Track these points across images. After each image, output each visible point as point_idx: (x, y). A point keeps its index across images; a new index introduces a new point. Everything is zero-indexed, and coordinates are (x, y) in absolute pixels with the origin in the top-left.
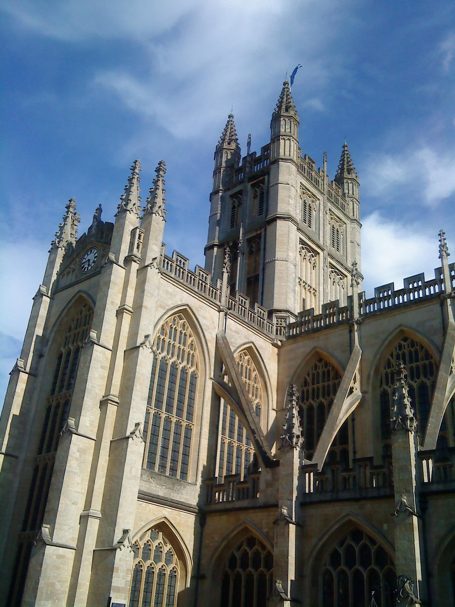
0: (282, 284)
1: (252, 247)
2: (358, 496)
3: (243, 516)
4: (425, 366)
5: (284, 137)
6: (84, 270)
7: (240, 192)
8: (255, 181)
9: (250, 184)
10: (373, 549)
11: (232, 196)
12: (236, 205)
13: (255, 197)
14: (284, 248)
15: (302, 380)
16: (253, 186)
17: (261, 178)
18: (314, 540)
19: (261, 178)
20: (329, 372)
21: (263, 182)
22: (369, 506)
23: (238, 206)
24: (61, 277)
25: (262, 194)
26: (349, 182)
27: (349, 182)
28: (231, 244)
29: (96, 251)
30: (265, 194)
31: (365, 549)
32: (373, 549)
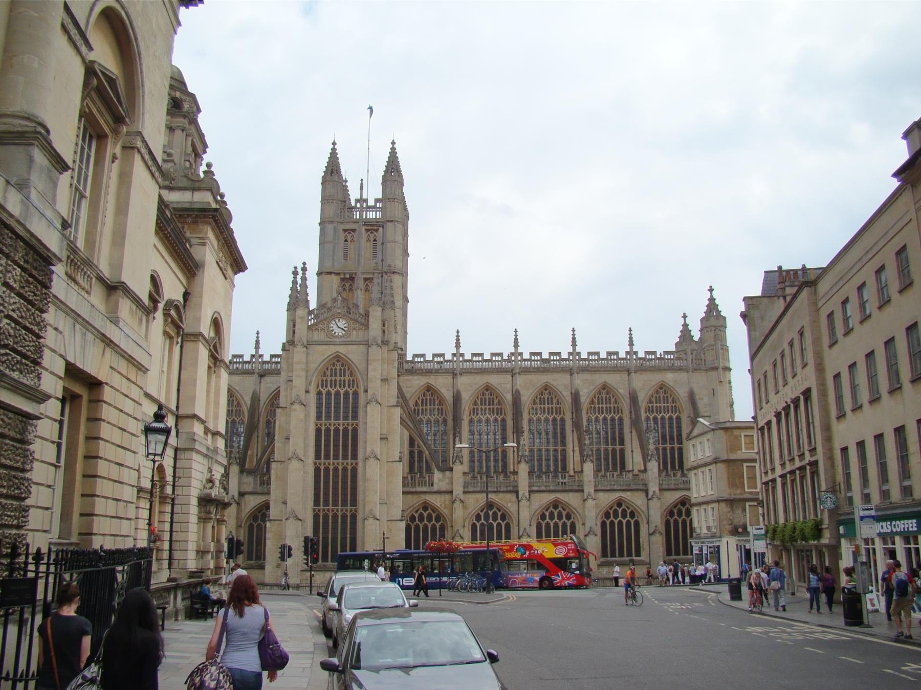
2: (495, 490)
3: (423, 497)
7: (354, 230)
8: (369, 228)
9: (364, 228)
10: (499, 514)
11: (345, 231)
12: (349, 240)
13: (368, 240)
15: (414, 401)
16: (367, 230)
17: (376, 228)
18: (470, 510)
19: (376, 228)
20: (434, 399)
21: (377, 230)
22: (501, 495)
25: (375, 240)
28: (348, 276)
29: (344, 322)
30: (379, 243)
31: (495, 514)
32: (499, 514)
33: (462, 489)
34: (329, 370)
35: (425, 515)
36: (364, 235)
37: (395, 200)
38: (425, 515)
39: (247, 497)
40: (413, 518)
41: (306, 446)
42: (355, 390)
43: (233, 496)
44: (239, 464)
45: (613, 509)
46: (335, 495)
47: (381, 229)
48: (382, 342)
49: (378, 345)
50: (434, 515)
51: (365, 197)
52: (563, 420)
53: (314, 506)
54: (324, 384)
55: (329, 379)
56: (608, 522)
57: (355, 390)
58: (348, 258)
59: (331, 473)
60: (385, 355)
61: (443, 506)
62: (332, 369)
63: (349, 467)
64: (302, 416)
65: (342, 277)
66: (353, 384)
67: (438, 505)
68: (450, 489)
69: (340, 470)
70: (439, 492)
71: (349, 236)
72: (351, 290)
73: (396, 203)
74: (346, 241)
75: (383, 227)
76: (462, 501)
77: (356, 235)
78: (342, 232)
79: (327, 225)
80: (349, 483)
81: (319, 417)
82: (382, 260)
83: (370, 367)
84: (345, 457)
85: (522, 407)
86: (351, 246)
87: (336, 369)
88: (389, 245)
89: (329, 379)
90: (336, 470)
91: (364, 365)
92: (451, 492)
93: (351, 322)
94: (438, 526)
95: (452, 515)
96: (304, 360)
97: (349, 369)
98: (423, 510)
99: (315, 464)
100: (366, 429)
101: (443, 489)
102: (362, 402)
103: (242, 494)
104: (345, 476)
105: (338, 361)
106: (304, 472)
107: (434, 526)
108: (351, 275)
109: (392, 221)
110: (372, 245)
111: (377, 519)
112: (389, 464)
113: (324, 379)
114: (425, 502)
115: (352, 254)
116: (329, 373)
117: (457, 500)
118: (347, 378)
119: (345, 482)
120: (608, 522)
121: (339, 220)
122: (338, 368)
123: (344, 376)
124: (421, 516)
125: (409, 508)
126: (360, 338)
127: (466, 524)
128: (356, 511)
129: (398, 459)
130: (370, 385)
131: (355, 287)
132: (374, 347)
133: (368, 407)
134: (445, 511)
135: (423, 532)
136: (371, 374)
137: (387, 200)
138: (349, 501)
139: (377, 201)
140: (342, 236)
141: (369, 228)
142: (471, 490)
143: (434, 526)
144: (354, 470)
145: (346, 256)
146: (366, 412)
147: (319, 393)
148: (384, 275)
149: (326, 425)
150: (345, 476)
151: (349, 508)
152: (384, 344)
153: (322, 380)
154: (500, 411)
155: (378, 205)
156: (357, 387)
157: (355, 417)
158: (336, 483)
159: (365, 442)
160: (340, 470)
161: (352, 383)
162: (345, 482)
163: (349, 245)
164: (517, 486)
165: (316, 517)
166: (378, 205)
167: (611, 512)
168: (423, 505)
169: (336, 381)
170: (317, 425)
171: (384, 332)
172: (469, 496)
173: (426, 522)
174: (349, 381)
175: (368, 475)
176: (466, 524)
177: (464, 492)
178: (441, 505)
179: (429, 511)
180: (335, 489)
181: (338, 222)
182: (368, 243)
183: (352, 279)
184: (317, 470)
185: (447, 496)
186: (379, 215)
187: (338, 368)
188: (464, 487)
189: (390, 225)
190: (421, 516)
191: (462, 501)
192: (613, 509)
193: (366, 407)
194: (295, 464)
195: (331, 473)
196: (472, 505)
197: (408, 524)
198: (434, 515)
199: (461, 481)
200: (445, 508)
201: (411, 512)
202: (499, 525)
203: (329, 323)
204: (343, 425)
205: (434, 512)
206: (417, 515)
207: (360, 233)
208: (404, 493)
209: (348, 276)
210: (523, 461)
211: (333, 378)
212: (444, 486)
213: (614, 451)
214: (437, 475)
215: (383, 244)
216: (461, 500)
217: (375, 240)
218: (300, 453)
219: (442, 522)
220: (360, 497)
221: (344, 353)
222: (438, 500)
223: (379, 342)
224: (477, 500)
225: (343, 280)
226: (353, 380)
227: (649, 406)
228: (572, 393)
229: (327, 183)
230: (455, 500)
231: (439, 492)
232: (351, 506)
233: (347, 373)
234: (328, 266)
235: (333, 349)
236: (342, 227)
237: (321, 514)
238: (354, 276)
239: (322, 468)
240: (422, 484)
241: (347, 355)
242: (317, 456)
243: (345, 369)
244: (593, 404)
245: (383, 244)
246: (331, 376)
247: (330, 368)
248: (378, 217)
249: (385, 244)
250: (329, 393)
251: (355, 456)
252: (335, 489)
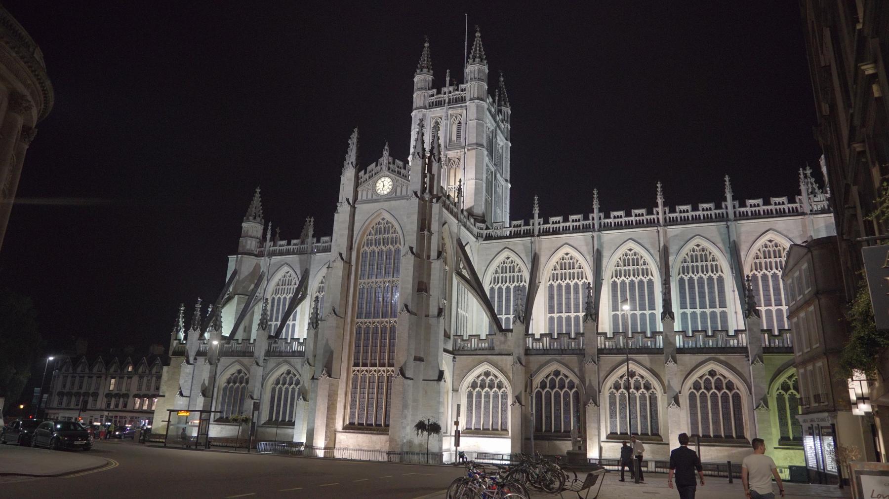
4: (578, 273)
30: (463, 124)
38: (488, 381)
45: (704, 378)
47: (465, 111)
52: (651, 283)
56: (698, 395)
94: (500, 393)
120: (698, 395)
167: (702, 382)
192: (704, 378)
202: (567, 395)
206: (479, 382)
213: (713, 314)
217: (460, 123)
227: (756, 263)
228: (659, 251)
244: (685, 262)
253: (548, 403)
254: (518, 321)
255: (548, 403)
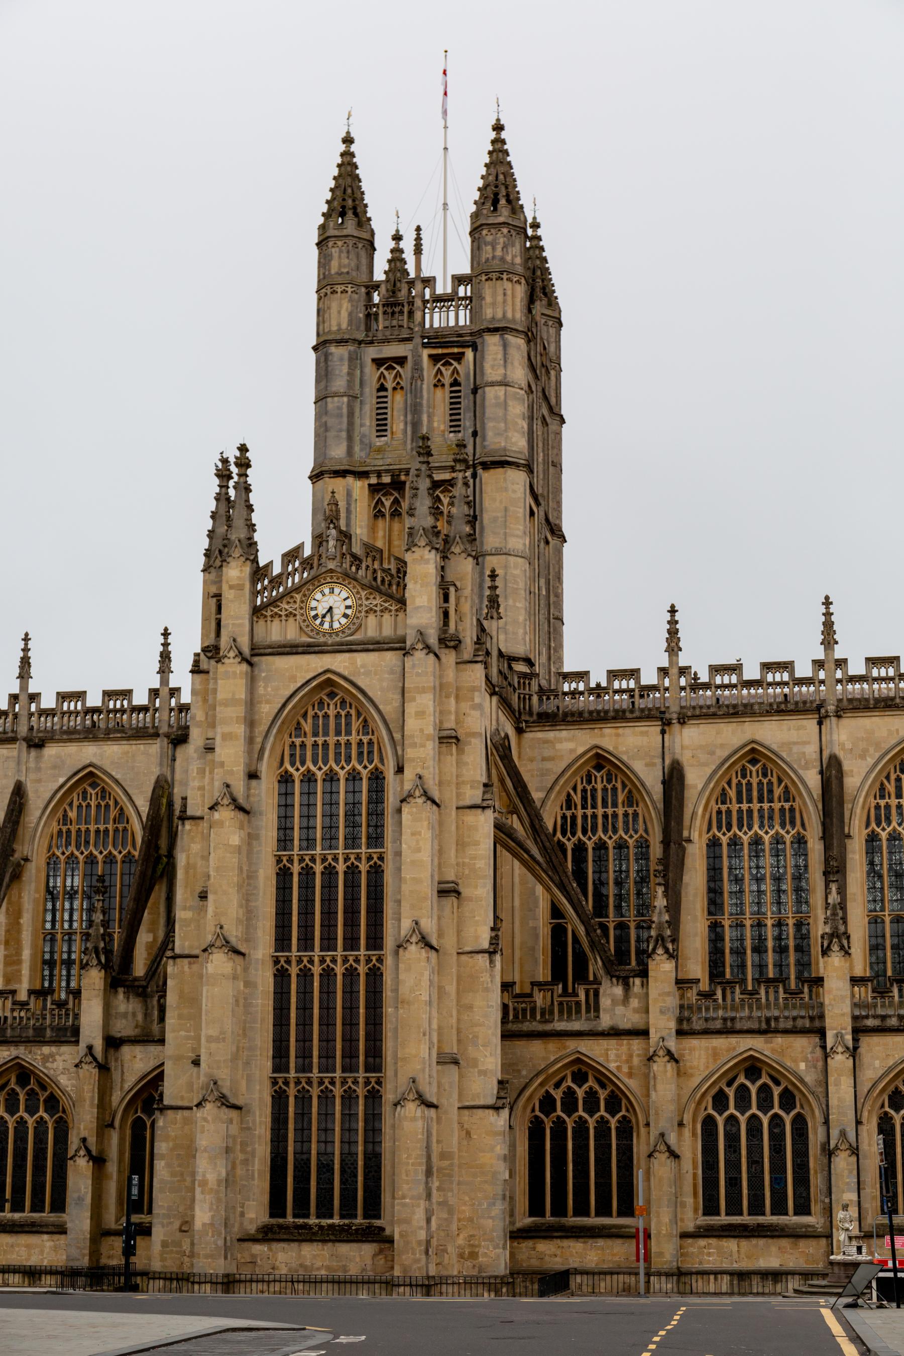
0: (518, 605)
1: (438, 499)
2: (764, 1026)
3: (572, 1045)
5: (511, 276)
6: (322, 624)
7: (401, 361)
8: (440, 351)
9: (425, 353)
11: (378, 362)
12: (390, 385)
13: (439, 384)
14: (519, 529)
16: (434, 358)
17: (456, 350)
19: (456, 350)
21: (459, 357)
23: (395, 389)
24: (255, 619)
25: (456, 383)
26: (550, 323)
27: (550, 323)
30: (465, 389)
33: (673, 1025)
34: (310, 720)
35: (580, 1093)
36: (428, 370)
37: (505, 276)
38: (580, 1093)
39: (127, 1051)
40: (547, 1103)
41: (249, 916)
42: (377, 769)
43: (90, 1048)
44: (106, 967)
46: (327, 1040)
47: (469, 354)
48: (442, 641)
49: (428, 648)
50: (603, 1095)
51: (425, 273)
53: (274, 1071)
54: (296, 754)
55: (309, 741)
57: (377, 769)
58: (388, 433)
59: (316, 984)
60: (450, 674)
61: (625, 1069)
62: (316, 716)
63: (362, 969)
64: (235, 839)
65: (373, 480)
66: (370, 753)
67: (612, 1066)
68: (642, 1026)
69: (339, 978)
70: (615, 1033)
71: (390, 376)
72: (396, 514)
73: (508, 285)
74: (382, 388)
75: (475, 348)
76: (671, 1056)
77: (406, 372)
78: (369, 367)
79: (333, 349)
80: (362, 1011)
81: (284, 842)
82: (475, 434)
83: (410, 709)
84: (351, 943)
85: (847, 806)
86: (397, 401)
87: (326, 716)
88: (492, 394)
89: (309, 741)
90: (328, 975)
91: (397, 704)
92: (643, 1033)
93: (363, 593)
94: (613, 1123)
95: (648, 1095)
96: (242, 695)
97: (359, 714)
98: (573, 1081)
99: (276, 961)
100: (399, 869)
101: (625, 1025)
102: (391, 799)
103: (113, 1043)
104: (350, 992)
105: (332, 695)
106: (247, 984)
107: (603, 1124)
108: (395, 475)
109: (496, 330)
110: (447, 395)
111: (430, 1105)
112: (464, 958)
113: (298, 741)
114: (578, 1061)
115: (398, 424)
116: (307, 727)
117: (661, 1053)
118: (354, 738)
119: (350, 1008)
121: (361, 336)
122: (332, 712)
123: (348, 733)
124: (570, 1095)
125: (537, 1075)
126: (388, 631)
127: (687, 1118)
128: (379, 1083)
129: (485, 945)
130: (410, 753)
131: (405, 505)
132: (420, 655)
133: (405, 816)
134: (632, 1085)
135: (573, 1139)
136: (411, 724)
137: (484, 278)
138: (362, 1058)
139: (459, 280)
140: (372, 374)
141: (440, 351)
142: (698, 1028)
143: (603, 1124)
144: (375, 976)
145: (382, 426)
146: (400, 823)
147: (285, 779)
148: (480, 471)
149: (301, 860)
150: (350, 992)
151: (361, 1075)
152: (447, 647)
153: (293, 746)
154: (790, 817)
155: (461, 291)
156: (382, 760)
157: (376, 839)
158: (327, 1008)
159: (399, 902)
160: (339, 978)
161: (368, 750)
162: (350, 1008)
163: (389, 399)
164: (822, 1017)
165: (279, 1099)
166: (461, 291)
168: (575, 1068)
169: (326, 745)
170: (279, 861)
171: (446, 614)
172: (694, 1042)
173: (581, 1112)
174: (360, 744)
175: (404, 990)
176: (687, 1118)
177: (680, 1033)
178: (618, 1068)
179: (591, 1082)
180: (327, 1022)
181: (360, 343)
182: (439, 392)
183: (398, 485)
184: (281, 976)
185: (636, 1044)
186: (463, 318)
187: (332, 712)
188: (680, 1020)
189: (492, 342)
190: (570, 1095)
191: (671, 1056)
193: (399, 811)
194: (219, 963)
195: (316, 984)
196: (702, 1068)
197: (536, 1117)
198: (603, 1095)
199: (672, 1001)
200: (630, 1075)
201: (542, 1084)
203: (306, 597)
204: (346, 859)
205: (603, 1086)
206: (558, 1095)
207: (418, 367)
208: (507, 1036)
209: (387, 479)
210: (835, 948)
211: (320, 740)
212: (626, 1017)
214: (611, 991)
215: (475, 391)
216: (669, 1053)
217: (456, 383)
218: (234, 934)
219: (623, 1113)
220: (388, 1046)
221: (346, 673)
222: (612, 1055)
223: (433, 641)
224: (715, 1054)
225: (374, 489)
226: (370, 743)
229: (330, 244)
230: (655, 1054)
231: (615, 1033)
232: (367, 1070)
233: (355, 725)
234: (338, 452)
235: (315, 664)
236: (372, 352)
237: (292, 1091)
238: (403, 478)
239: (294, 970)
240: (570, 1010)
241: (352, 678)
242: (282, 940)
243: (348, 715)
245: (475, 391)
246: (315, 734)
247: (311, 713)
248: (461, 323)
249: (480, 391)
250: (309, 778)
251: (376, 941)
252: (327, 1022)
253: (732, 1140)
254: (660, 951)
255: (732, 1140)
